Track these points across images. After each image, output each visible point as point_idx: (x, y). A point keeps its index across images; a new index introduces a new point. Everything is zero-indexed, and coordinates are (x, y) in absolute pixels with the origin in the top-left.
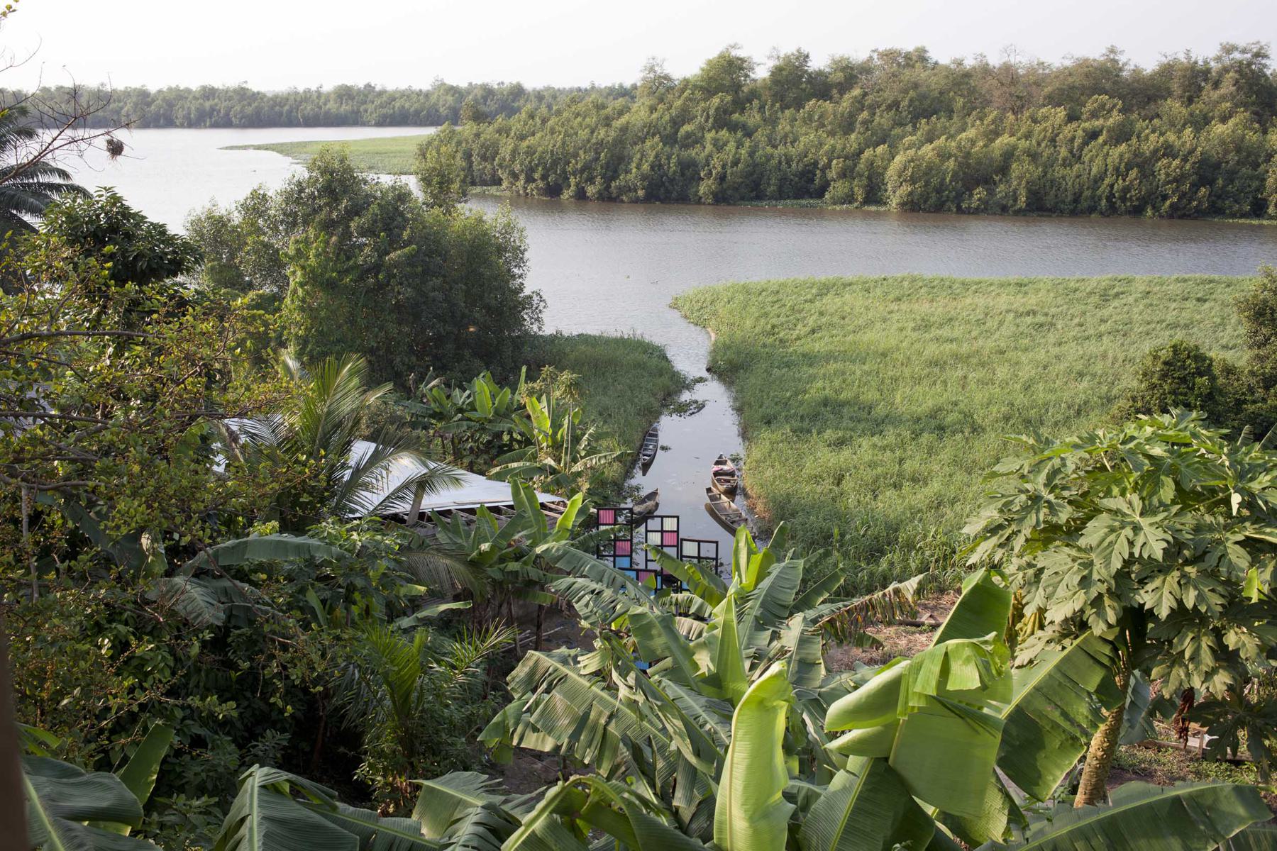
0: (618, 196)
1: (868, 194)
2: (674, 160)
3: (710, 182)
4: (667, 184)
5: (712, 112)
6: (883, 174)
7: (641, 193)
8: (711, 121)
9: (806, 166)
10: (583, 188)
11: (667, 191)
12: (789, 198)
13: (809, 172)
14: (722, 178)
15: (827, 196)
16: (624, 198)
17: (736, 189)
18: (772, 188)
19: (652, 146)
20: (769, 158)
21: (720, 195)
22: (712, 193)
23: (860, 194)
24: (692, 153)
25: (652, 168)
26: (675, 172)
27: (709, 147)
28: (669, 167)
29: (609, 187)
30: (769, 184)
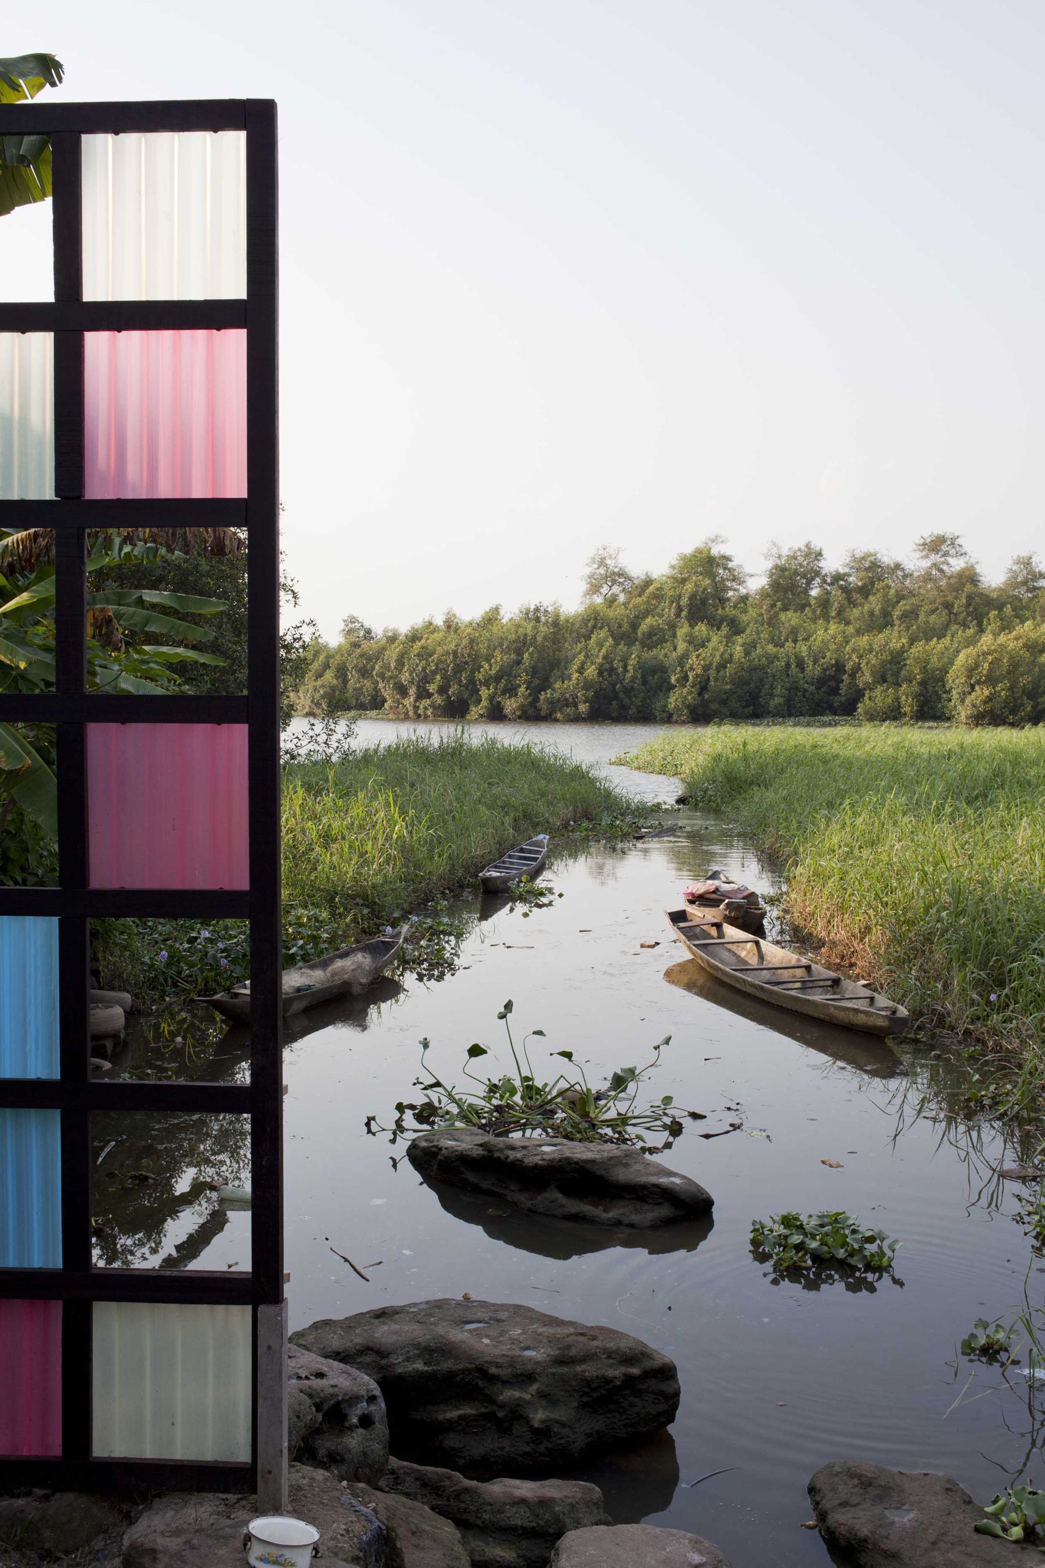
0: (550, 715)
1: (922, 707)
2: (632, 662)
3: (685, 691)
4: (621, 695)
5: (684, 601)
6: (942, 680)
7: (583, 708)
8: (684, 614)
9: (825, 670)
10: (499, 703)
11: (623, 707)
12: (802, 715)
13: (832, 678)
14: (703, 686)
15: (861, 708)
16: (559, 715)
17: (724, 702)
18: (777, 700)
19: (601, 643)
20: (772, 659)
21: (700, 711)
22: (688, 707)
23: (908, 706)
24: (658, 653)
25: (600, 673)
26: (633, 679)
27: (681, 646)
28: (626, 670)
29: (537, 700)
30: (772, 695)
